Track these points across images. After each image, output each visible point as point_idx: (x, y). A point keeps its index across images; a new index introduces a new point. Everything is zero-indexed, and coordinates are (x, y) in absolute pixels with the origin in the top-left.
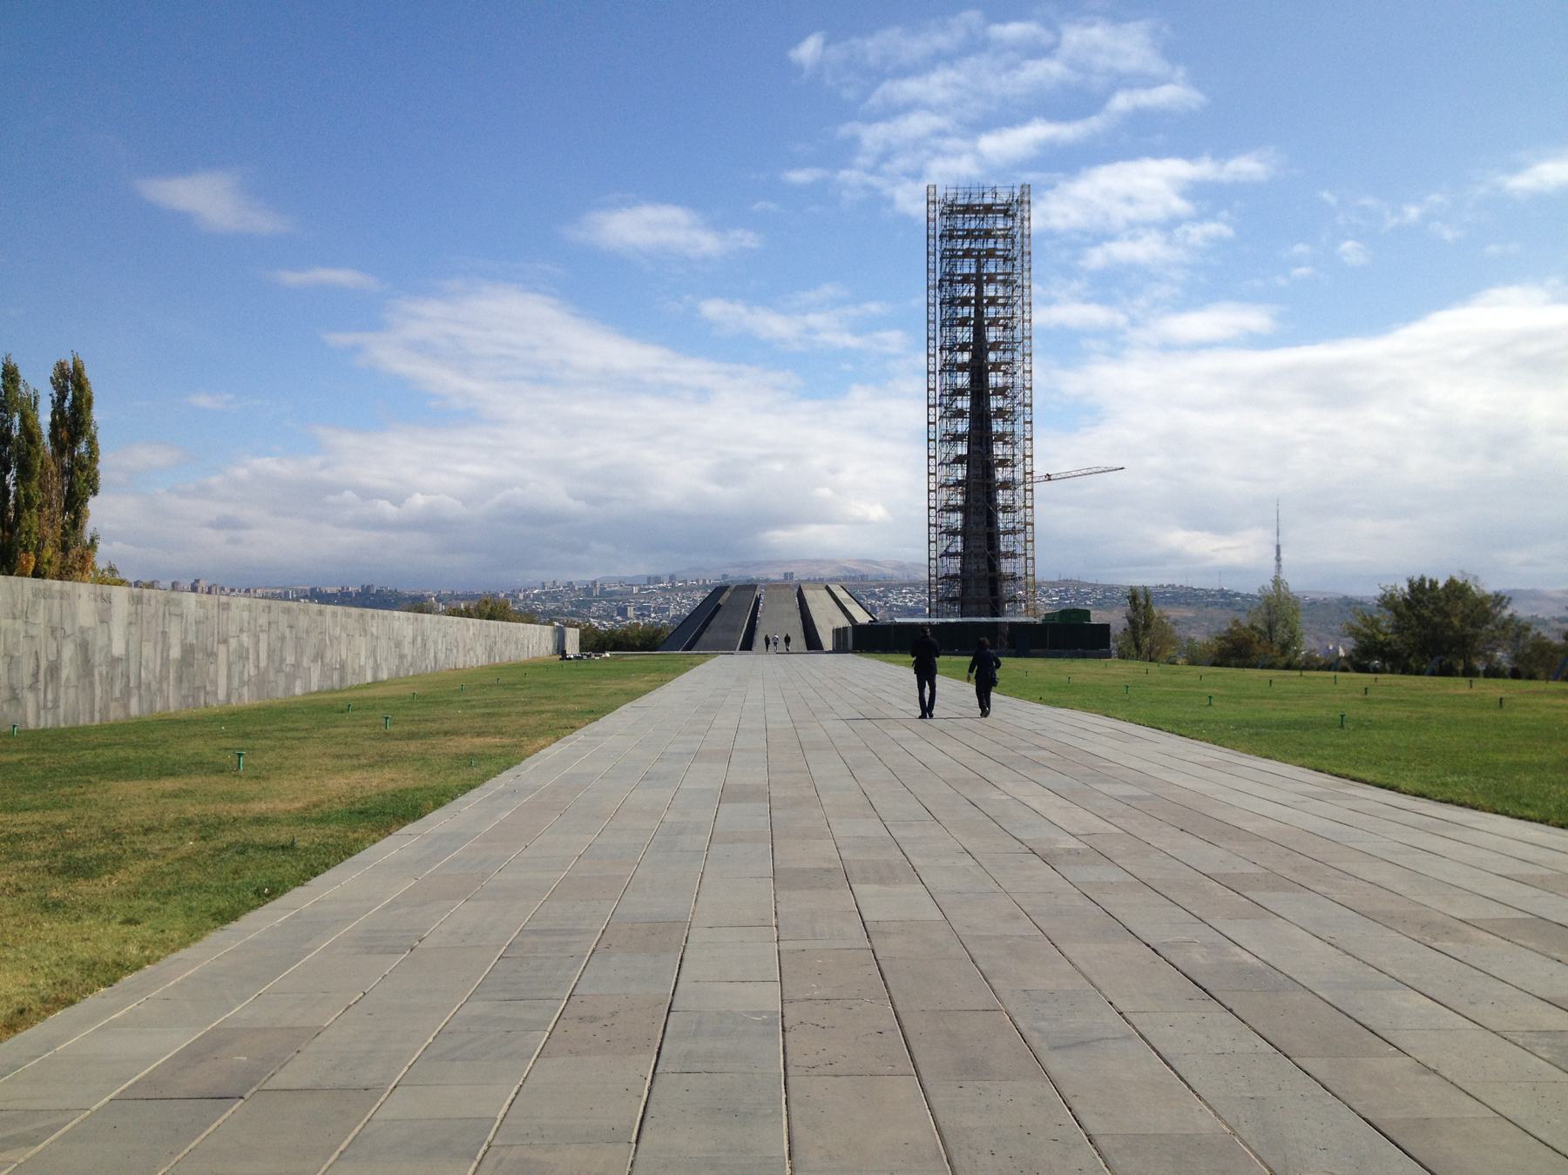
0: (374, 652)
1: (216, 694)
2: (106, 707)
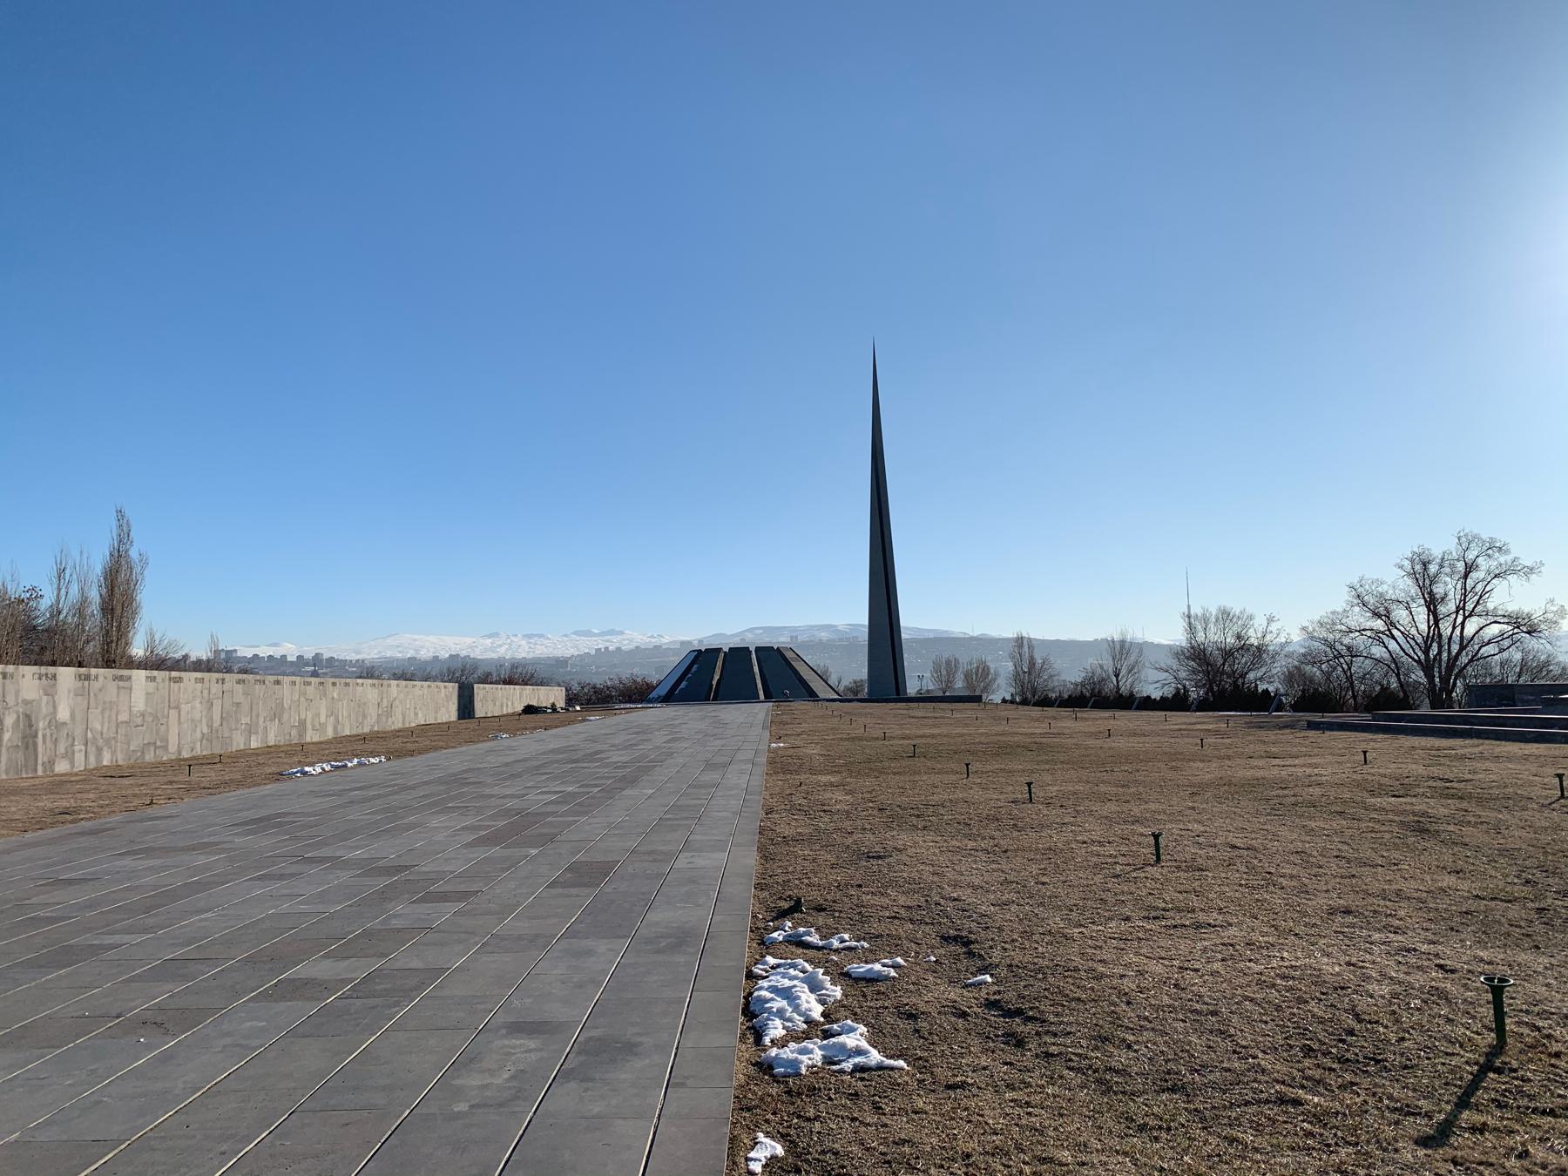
0: (332, 713)
1: (165, 748)
2: (51, 763)
